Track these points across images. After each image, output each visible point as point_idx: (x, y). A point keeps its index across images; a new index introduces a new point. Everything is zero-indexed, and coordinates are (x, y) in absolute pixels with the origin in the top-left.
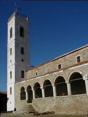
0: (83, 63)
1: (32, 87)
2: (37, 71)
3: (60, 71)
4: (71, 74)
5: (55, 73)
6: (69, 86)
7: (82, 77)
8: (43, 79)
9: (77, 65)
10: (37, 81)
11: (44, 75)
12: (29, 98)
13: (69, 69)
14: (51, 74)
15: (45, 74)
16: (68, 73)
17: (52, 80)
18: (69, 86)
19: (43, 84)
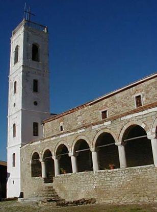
0: (146, 108)
1: (53, 153)
2: (61, 124)
3: (105, 124)
4: (126, 127)
5: (96, 127)
6: (121, 151)
7: (146, 134)
9: (135, 111)
11: (74, 130)
12: (47, 174)
13: (122, 119)
15: (78, 129)
17: (91, 140)
18: (121, 151)
19: (73, 148)
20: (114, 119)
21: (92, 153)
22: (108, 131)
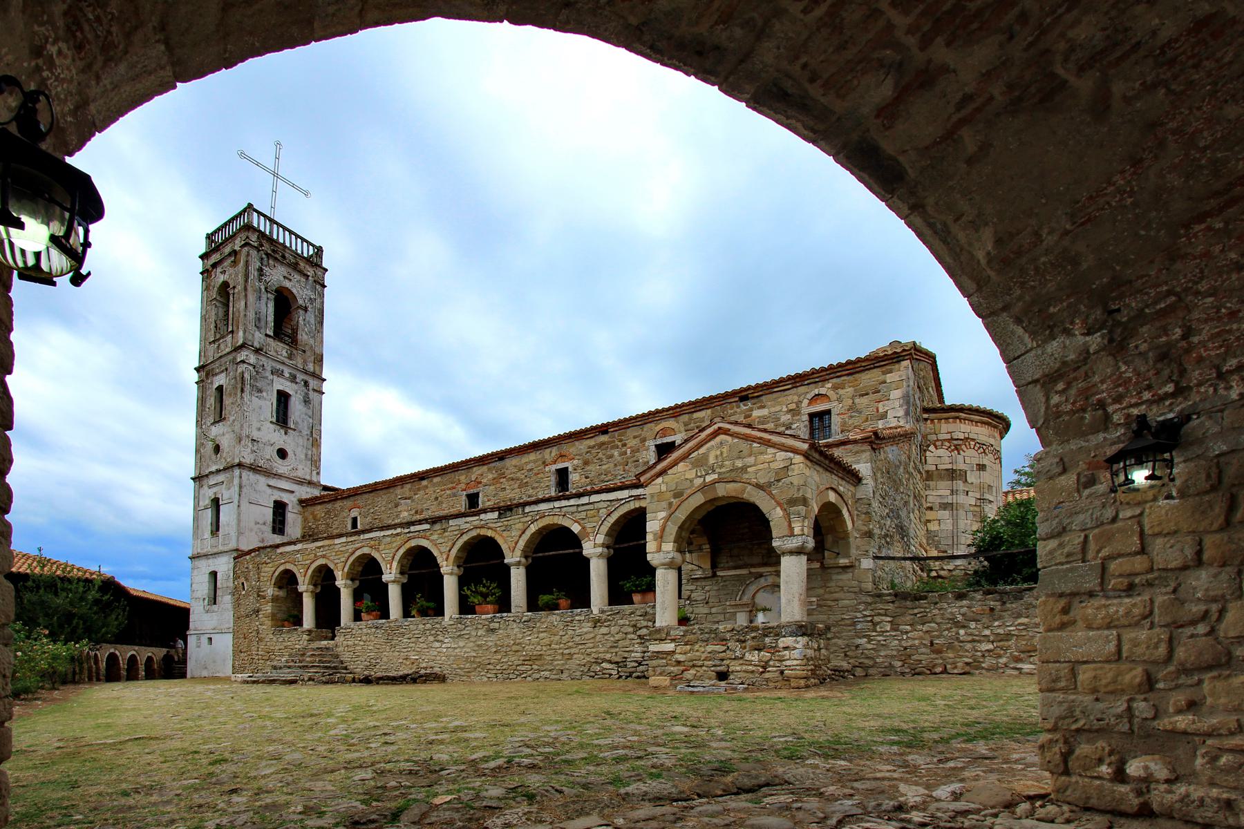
1: (338, 574)
4: (533, 528)
6: (518, 579)
8: (399, 540)
10: (366, 550)
11: (401, 525)
13: (527, 509)
14: (437, 526)
16: (520, 526)
17: (444, 549)
18: (518, 579)
20: (505, 510)
21: (446, 577)
22: (489, 533)
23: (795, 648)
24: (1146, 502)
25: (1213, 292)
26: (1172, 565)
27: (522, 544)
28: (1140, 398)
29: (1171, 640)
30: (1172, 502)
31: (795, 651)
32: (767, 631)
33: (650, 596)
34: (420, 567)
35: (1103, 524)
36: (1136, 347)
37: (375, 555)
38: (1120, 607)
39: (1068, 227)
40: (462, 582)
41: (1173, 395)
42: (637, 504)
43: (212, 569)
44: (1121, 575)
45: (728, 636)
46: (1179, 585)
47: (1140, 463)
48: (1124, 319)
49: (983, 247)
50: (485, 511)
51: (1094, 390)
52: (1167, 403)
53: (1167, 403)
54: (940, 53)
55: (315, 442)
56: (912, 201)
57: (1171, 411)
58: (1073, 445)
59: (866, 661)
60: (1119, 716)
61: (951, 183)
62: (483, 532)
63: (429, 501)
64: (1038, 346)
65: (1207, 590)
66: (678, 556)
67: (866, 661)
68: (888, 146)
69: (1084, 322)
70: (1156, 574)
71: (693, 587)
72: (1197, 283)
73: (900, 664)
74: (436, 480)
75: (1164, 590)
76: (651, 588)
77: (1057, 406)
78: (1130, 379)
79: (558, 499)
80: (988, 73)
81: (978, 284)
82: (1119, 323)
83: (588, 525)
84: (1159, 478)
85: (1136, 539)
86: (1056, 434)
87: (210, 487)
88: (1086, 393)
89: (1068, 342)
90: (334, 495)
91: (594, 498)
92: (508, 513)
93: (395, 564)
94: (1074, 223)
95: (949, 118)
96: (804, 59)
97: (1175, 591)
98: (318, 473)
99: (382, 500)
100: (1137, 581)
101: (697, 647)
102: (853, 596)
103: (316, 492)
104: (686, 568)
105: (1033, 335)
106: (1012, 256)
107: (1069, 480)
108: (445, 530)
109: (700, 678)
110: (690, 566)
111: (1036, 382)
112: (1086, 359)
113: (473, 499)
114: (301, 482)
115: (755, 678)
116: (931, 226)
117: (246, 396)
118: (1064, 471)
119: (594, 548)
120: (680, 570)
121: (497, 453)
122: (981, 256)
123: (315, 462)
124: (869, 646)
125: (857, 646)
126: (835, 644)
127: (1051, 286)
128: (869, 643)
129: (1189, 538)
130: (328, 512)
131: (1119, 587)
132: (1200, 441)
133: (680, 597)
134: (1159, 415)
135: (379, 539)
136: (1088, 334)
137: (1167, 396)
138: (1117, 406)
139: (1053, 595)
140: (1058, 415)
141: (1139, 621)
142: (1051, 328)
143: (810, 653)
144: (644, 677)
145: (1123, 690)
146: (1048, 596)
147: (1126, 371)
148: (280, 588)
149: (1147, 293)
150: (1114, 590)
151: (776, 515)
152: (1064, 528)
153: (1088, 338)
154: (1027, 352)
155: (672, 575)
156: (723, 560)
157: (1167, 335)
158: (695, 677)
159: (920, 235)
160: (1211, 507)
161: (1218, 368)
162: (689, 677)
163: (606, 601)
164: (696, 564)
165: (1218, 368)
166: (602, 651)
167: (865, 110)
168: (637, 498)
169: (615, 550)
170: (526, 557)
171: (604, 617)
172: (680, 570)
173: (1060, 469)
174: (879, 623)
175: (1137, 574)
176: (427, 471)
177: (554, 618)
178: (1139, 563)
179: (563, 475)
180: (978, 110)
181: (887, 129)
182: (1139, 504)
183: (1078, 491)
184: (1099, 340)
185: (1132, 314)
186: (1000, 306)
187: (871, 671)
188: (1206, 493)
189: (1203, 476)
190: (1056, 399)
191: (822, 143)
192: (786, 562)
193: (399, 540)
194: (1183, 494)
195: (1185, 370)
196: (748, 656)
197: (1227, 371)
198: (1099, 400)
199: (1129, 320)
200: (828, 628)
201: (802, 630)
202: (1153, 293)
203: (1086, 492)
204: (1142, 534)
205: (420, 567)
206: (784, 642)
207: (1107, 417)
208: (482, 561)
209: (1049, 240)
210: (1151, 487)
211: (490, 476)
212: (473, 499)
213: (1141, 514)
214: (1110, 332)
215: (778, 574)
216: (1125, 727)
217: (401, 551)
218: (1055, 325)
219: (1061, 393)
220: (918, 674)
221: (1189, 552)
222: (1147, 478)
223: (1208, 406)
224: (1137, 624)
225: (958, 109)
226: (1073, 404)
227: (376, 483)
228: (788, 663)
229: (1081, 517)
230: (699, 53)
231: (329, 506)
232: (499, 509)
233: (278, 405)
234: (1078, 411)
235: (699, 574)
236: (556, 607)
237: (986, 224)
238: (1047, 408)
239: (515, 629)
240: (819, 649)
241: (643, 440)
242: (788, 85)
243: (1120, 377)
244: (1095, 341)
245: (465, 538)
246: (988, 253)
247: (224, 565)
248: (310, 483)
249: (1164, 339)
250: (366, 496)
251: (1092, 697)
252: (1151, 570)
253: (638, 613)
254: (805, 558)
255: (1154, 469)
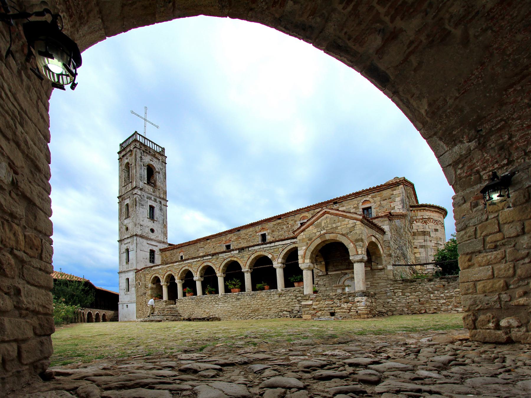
1: (176, 278)
4: (253, 257)
5: (224, 255)
6: (248, 278)
8: (199, 263)
10: (187, 268)
13: (250, 249)
14: (214, 257)
16: (247, 256)
17: (218, 266)
18: (248, 278)
20: (241, 250)
21: (219, 278)
22: (235, 259)
23: (362, 302)
24: (499, 210)
25: (519, 118)
26: (512, 235)
27: (248, 263)
28: (494, 167)
29: (514, 267)
30: (510, 209)
31: (362, 303)
32: (350, 295)
33: (301, 283)
34: (209, 274)
35: (482, 222)
36: (490, 145)
37: (190, 269)
38: (492, 256)
39: (457, 95)
40: (225, 280)
41: (507, 164)
42: (294, 246)
43: (127, 277)
44: (491, 242)
45: (334, 297)
46: (516, 243)
47: (495, 191)
48: (484, 134)
49: (424, 108)
50: (233, 250)
51: (474, 166)
52: (505, 168)
53: (505, 168)
54: (399, 23)
55: (165, 226)
56: (393, 90)
57: (507, 171)
58: (468, 191)
59: (392, 309)
60: (495, 302)
61: (408, 81)
62: (233, 259)
63: (210, 248)
64: (450, 149)
65: (528, 244)
66: (312, 265)
67: (392, 309)
68: (382, 66)
69: (467, 136)
70: (506, 240)
71: (318, 279)
72: (512, 115)
73: (406, 309)
74: (213, 240)
75: (510, 246)
76: (301, 280)
77: (460, 174)
78: (488, 159)
79: (262, 244)
80: (419, 31)
81: (423, 124)
82: (482, 136)
83: (275, 255)
84: (503, 196)
85: (496, 226)
86: (460, 187)
87: (125, 244)
88: (471, 168)
89: (462, 146)
90: (172, 247)
91: (277, 243)
92: (242, 251)
93: (198, 273)
94: (459, 93)
95: (405, 52)
96: (345, 30)
97: (514, 246)
98: (167, 239)
99: (192, 249)
100: (498, 244)
101: (321, 302)
102: (385, 281)
103: (166, 246)
104: (315, 271)
105: (447, 144)
106: (436, 110)
107: (467, 206)
108: (217, 258)
109: (324, 315)
110: (317, 271)
111: (450, 165)
112: (470, 153)
113: (228, 247)
114: (160, 242)
115: (346, 314)
116: (402, 100)
117: (137, 207)
118: (465, 202)
119: (278, 264)
120: (313, 271)
121: (237, 228)
122: (423, 112)
123: (165, 234)
124: (393, 302)
125: (388, 302)
126: (379, 302)
127: (453, 122)
128: (393, 301)
129: (518, 223)
130: (171, 254)
131: (491, 247)
132: (520, 182)
133: (313, 284)
134: (501, 174)
135: (191, 263)
136: (470, 142)
137: (504, 165)
138: (484, 172)
139: (464, 254)
140: (460, 178)
141: (501, 260)
142: (454, 141)
143: (368, 304)
144: (301, 317)
145: (496, 290)
146: (462, 255)
147: (487, 156)
148: (154, 284)
149: (492, 122)
150: (489, 249)
151: (350, 246)
152: (467, 226)
153: (470, 144)
154: (445, 152)
155: (310, 273)
156: (330, 267)
157: (502, 139)
158: (321, 315)
159: (398, 105)
160: (526, 208)
161: (524, 151)
162: (319, 315)
163: (284, 286)
164: (319, 270)
165: (524, 151)
166: (283, 307)
167: (371, 51)
168: (294, 243)
169: (286, 265)
170: (250, 269)
171: (283, 292)
172: (313, 271)
173: (463, 202)
174: (396, 292)
175: (498, 241)
176: (209, 236)
177: (263, 293)
178: (498, 236)
179: (264, 236)
180: (417, 47)
181: (380, 58)
182: (496, 212)
183: (471, 210)
184: (474, 144)
185: (487, 131)
186: (433, 133)
187: (394, 313)
188: (524, 203)
189: (522, 196)
190: (459, 172)
191: (355, 67)
192: (356, 266)
193: (199, 263)
194: (514, 205)
195: (511, 153)
196: (343, 306)
197: (529, 152)
198: (477, 170)
199: (486, 134)
200: (375, 294)
201: (364, 294)
202: (494, 121)
203: (475, 209)
204: (499, 223)
205: (209, 274)
206: (357, 299)
207: (481, 177)
208: (233, 271)
209: (450, 102)
210: (501, 201)
211: (235, 238)
212: (228, 247)
213: (498, 216)
214: (479, 140)
215: (353, 273)
216: (498, 306)
217: (201, 268)
218: (456, 140)
219: (461, 169)
220: (415, 314)
221: (519, 229)
222: (498, 196)
223: (522, 167)
224: (500, 262)
225: (408, 48)
226: (466, 173)
227: (189, 242)
228: (359, 308)
229: (473, 220)
230: (304, 30)
231: (172, 251)
232: (239, 249)
233: (150, 211)
234: (468, 176)
235: (321, 274)
236: (264, 289)
237: (424, 97)
238: (456, 176)
239: (248, 298)
240: (372, 302)
241: (296, 221)
242: (339, 42)
243: (484, 159)
244: (473, 145)
245: (226, 261)
246: (426, 110)
247: (131, 276)
248: (164, 242)
249: (501, 140)
250: (186, 247)
251: (483, 295)
252: (504, 238)
253: (297, 290)
254: (363, 264)
255: (500, 193)
